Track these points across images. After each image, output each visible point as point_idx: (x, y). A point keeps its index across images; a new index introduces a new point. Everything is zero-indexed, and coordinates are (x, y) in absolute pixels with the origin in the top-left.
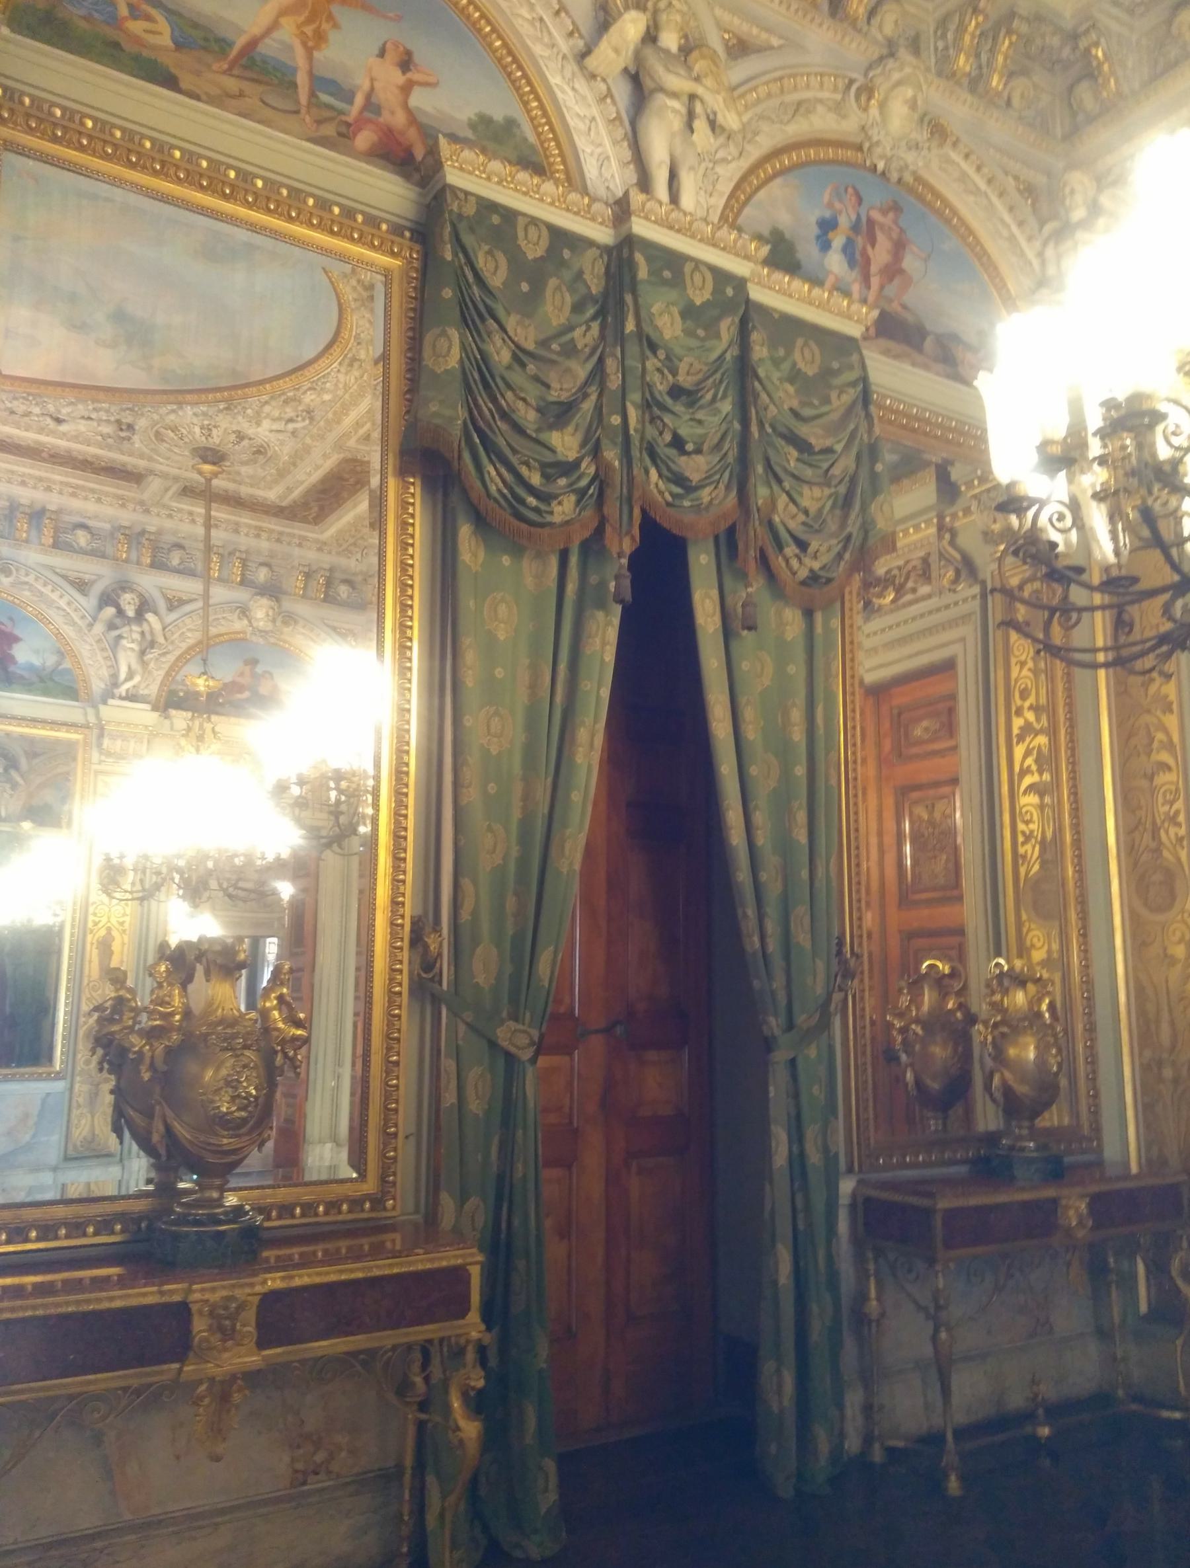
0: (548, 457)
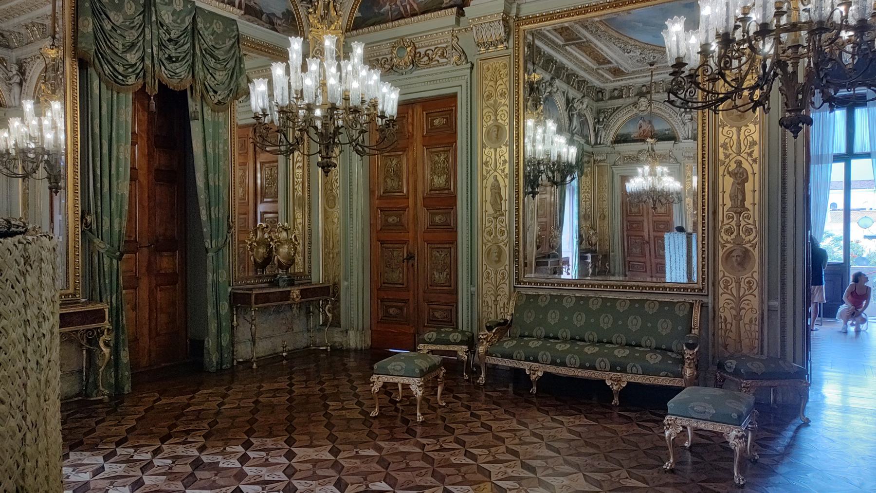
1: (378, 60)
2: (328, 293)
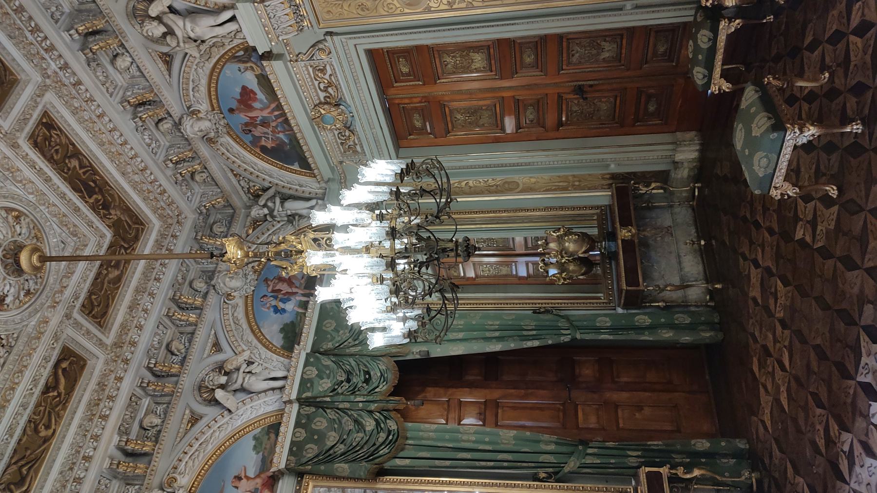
0: (376, 431)
1: (342, 144)
2: (624, 186)
